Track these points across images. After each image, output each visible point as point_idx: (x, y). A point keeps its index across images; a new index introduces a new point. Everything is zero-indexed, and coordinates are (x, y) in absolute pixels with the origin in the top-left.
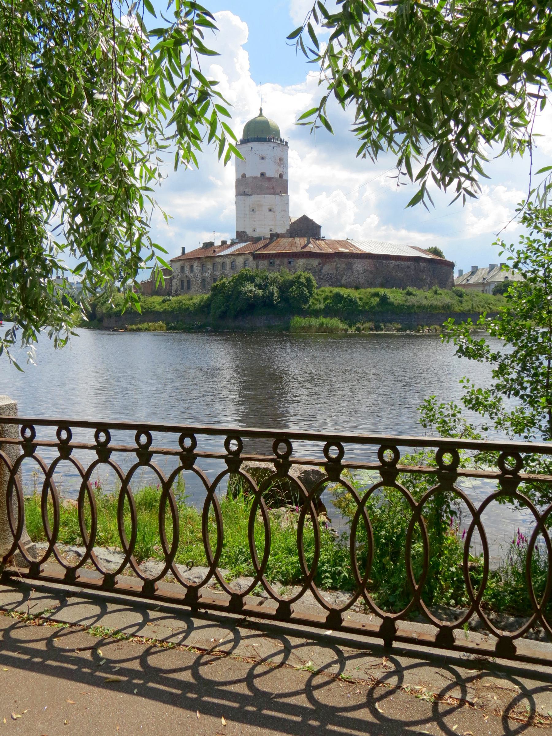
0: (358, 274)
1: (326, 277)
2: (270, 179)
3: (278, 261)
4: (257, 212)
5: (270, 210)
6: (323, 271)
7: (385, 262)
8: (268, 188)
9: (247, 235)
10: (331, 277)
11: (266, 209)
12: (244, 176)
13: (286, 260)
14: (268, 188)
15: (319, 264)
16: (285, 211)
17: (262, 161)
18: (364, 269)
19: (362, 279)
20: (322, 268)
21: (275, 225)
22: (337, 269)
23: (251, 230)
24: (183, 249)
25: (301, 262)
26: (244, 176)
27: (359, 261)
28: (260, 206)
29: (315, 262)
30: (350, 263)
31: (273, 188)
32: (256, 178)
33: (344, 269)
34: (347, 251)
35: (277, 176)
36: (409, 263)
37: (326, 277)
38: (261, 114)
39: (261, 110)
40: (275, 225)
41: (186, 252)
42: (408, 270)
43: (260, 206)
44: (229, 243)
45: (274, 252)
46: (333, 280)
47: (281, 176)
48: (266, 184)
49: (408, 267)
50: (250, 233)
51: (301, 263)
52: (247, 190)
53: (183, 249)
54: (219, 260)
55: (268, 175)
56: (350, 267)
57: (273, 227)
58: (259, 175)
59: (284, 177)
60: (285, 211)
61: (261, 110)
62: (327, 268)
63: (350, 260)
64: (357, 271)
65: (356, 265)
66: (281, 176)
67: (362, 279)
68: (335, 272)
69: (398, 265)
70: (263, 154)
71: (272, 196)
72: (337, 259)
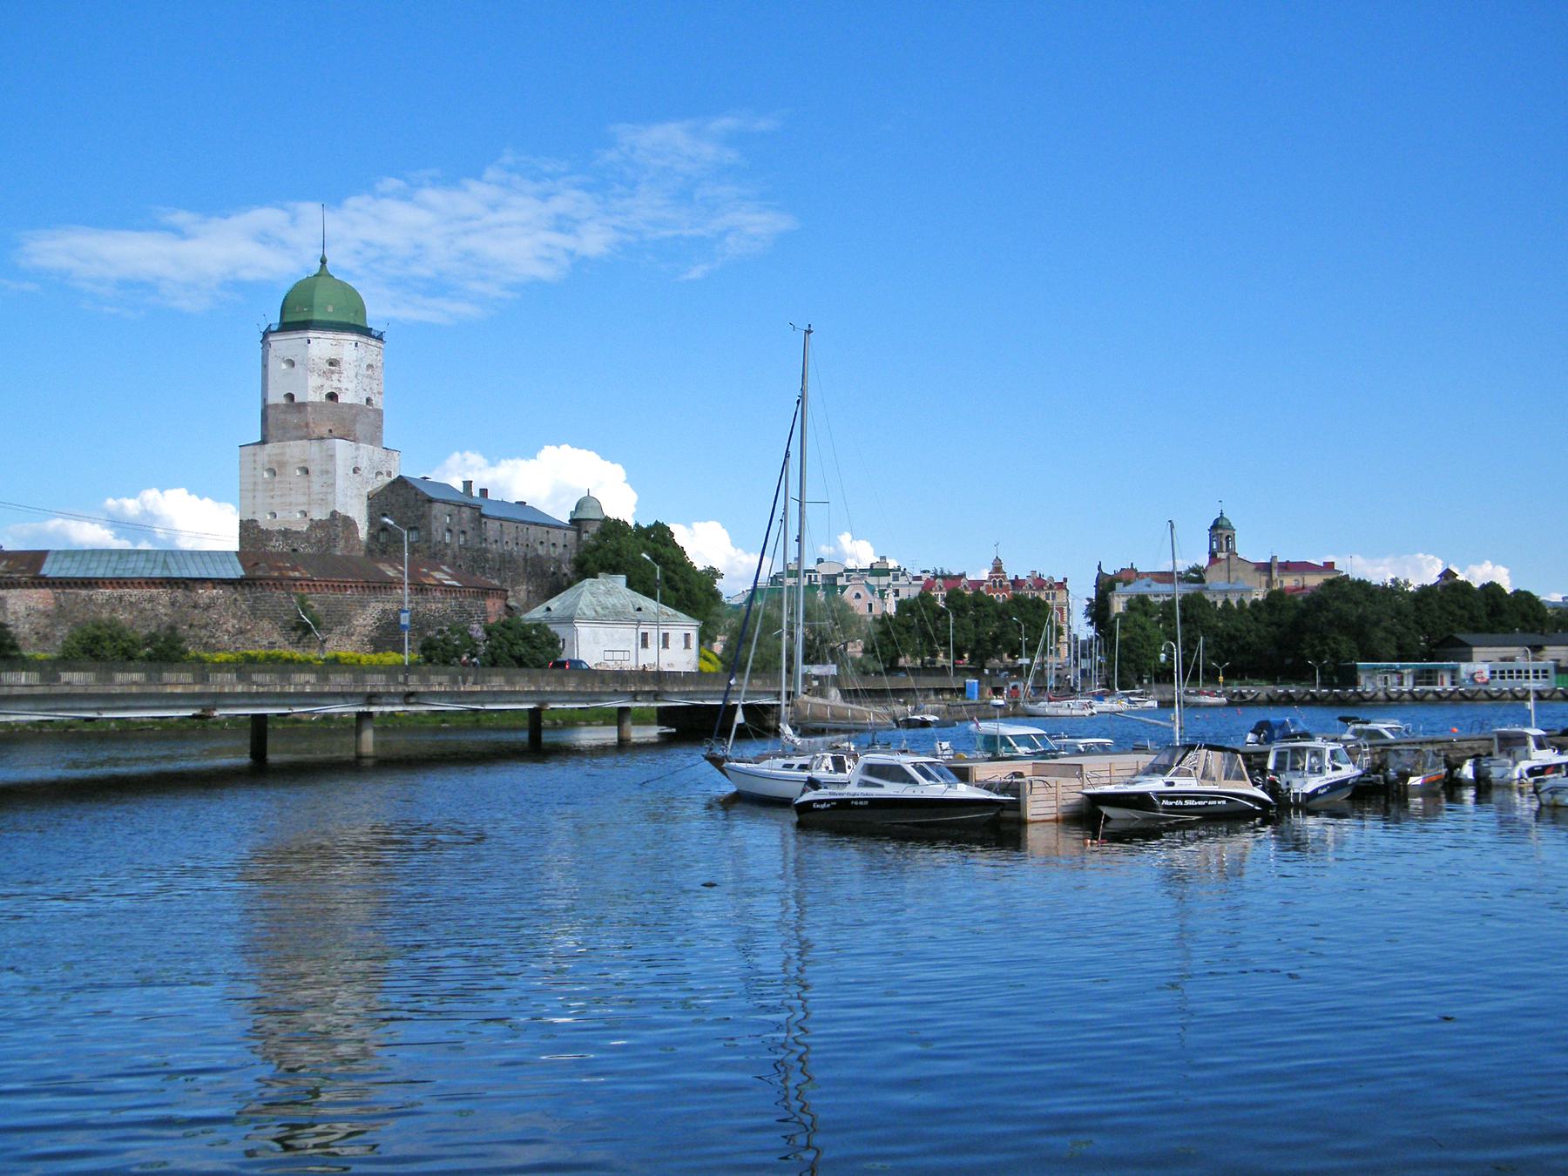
0: (17, 619)
7: (84, 592)
8: (298, 427)
16: (327, 472)
18: (28, 608)
28: (282, 464)
31: (307, 425)
32: (277, 405)
36: (154, 591)
39: (323, 261)
42: (148, 606)
43: (282, 464)
47: (332, 396)
48: (294, 419)
49: (151, 600)
50: (265, 521)
57: (304, 508)
60: (327, 472)
61: (323, 261)
64: (14, 613)
66: (332, 396)
69: (121, 598)
71: (304, 442)
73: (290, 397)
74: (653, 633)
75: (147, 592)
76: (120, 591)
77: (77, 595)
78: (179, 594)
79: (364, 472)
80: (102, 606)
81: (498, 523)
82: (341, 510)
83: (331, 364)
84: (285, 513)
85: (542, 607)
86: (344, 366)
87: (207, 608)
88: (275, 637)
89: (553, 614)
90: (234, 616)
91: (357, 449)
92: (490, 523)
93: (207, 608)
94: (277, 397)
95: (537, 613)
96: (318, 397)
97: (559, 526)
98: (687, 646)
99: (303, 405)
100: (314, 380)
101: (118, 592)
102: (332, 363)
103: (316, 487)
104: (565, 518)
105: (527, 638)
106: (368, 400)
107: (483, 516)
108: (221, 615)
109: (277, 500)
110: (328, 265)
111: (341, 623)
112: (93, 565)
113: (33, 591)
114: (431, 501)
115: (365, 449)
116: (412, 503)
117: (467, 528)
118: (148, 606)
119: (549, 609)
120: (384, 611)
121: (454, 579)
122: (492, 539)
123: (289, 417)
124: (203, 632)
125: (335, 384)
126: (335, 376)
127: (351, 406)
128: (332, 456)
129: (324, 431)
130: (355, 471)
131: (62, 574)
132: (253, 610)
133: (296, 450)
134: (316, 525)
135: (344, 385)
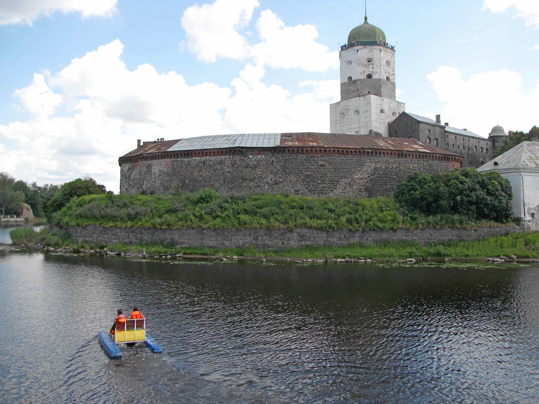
6: (131, 176)
7: (186, 160)
8: (354, 92)
11: (352, 112)
14: (354, 92)
15: (129, 169)
16: (367, 111)
18: (160, 171)
20: (131, 173)
27: (154, 162)
28: (347, 110)
31: (358, 90)
35: (363, 77)
36: (223, 157)
39: (366, 19)
40: (360, 128)
42: (219, 167)
46: (138, 186)
47: (369, 76)
48: (352, 88)
49: (221, 163)
57: (357, 130)
59: (374, 77)
60: (367, 111)
61: (366, 19)
63: (149, 162)
64: (155, 174)
65: (154, 167)
66: (369, 76)
69: (204, 162)
71: (357, 98)
73: (350, 78)
75: (219, 158)
76: (204, 158)
77: (183, 162)
78: (237, 158)
79: (386, 111)
80: (194, 168)
81: (454, 136)
83: (369, 61)
85: (492, 163)
86: (375, 61)
87: (254, 167)
88: (299, 186)
89: (500, 167)
90: (272, 173)
91: (383, 100)
92: (449, 135)
93: (254, 167)
95: (488, 167)
97: (484, 139)
99: (356, 81)
100: (361, 69)
102: (369, 61)
103: (362, 119)
104: (486, 136)
105: (483, 185)
106: (388, 78)
107: (446, 131)
108: (263, 172)
109: (346, 127)
110: (368, 21)
111: (345, 177)
112: (195, 144)
113: (162, 160)
114: (419, 122)
115: (386, 100)
116: (409, 125)
117: (438, 138)
118: (219, 167)
119: (496, 164)
120: (375, 169)
121: (426, 149)
122: (451, 144)
123: (350, 88)
124: (252, 183)
125: (371, 70)
126: (371, 66)
127: (379, 80)
129: (367, 92)
130: (382, 111)
132: (284, 168)
135: (375, 70)
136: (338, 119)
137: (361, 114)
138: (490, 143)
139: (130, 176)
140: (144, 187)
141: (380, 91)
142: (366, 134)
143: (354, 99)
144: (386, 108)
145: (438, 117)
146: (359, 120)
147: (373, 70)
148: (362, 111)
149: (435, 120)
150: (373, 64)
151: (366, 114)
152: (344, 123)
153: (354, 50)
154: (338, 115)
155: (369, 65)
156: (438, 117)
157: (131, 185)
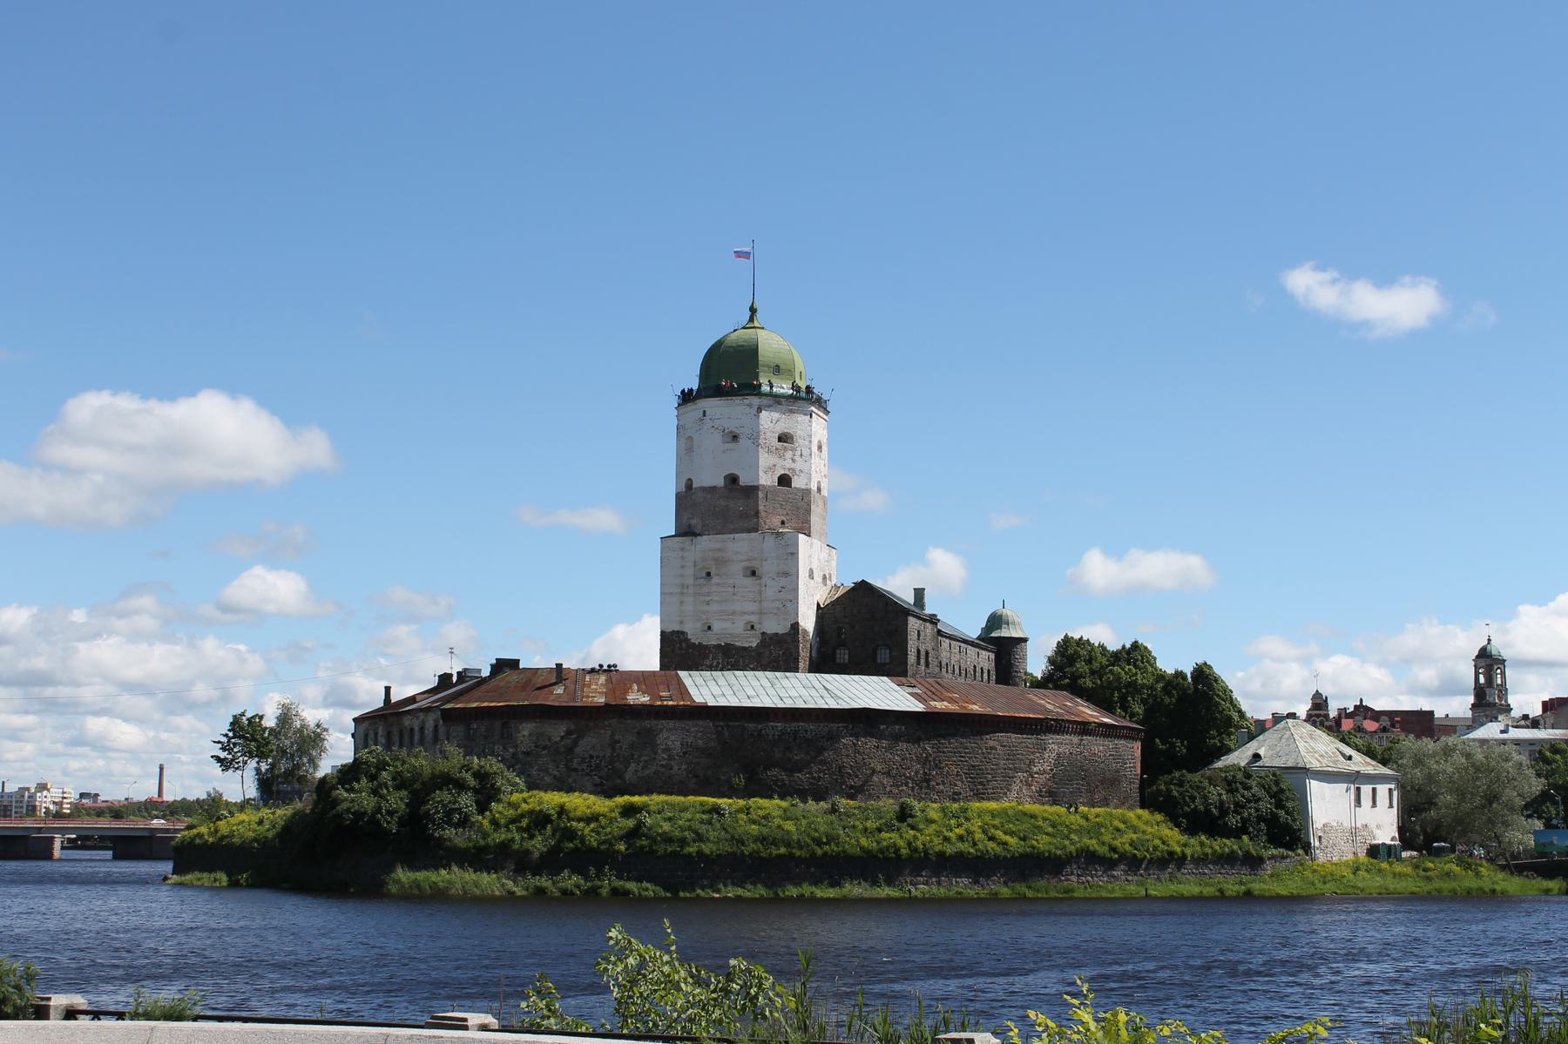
0: (670, 758)
1: (584, 766)
2: (752, 491)
3: (479, 727)
4: (715, 580)
5: (754, 573)
6: (577, 750)
7: (751, 726)
8: (744, 516)
9: (687, 640)
10: (598, 766)
11: (736, 569)
12: (689, 485)
13: (498, 724)
15: (569, 733)
16: (786, 574)
17: (731, 445)
19: (679, 770)
20: (575, 743)
21: (760, 613)
22: (613, 744)
23: (699, 625)
24: (388, 689)
25: (526, 730)
26: (689, 485)
27: (671, 724)
28: (721, 562)
29: (557, 731)
30: (649, 731)
31: (757, 514)
32: (713, 489)
33: (632, 746)
34: (645, 699)
36: (834, 726)
37: (584, 766)
38: (751, 320)
39: (753, 310)
40: (760, 613)
41: (394, 698)
43: (721, 562)
44: (455, 679)
45: (474, 705)
47: (784, 480)
48: (740, 505)
51: (526, 733)
52: (693, 522)
53: (388, 689)
54: (407, 721)
55: (743, 481)
56: (647, 740)
57: (754, 619)
58: (720, 482)
59: (797, 483)
60: (786, 574)
61: (753, 310)
62: (590, 743)
64: (667, 750)
66: (784, 480)
67: (679, 770)
68: (608, 752)
69: (795, 734)
70: (732, 426)
72: (614, 722)
73: (732, 480)
74: (1366, 790)
75: (824, 727)
82: (802, 623)
84: (727, 625)
89: (1266, 762)
94: (711, 477)
96: (767, 480)
97: (972, 644)
98: (1391, 806)
101: (792, 726)
103: (770, 592)
107: (939, 633)
109: (714, 607)
110: (758, 314)
119: (1257, 757)
120: (1059, 754)
126: (789, 454)
128: (794, 555)
130: (811, 576)
131: (722, 702)
133: (739, 545)
134: (769, 640)
135: (799, 465)
136: (690, 581)
137: (765, 580)
138: (992, 656)
139: (570, 750)
140: (628, 776)
141: (808, 522)
142: (781, 632)
143: (744, 535)
144: (814, 567)
145: (919, 593)
146: (760, 593)
147: (793, 466)
148: (768, 569)
149: (912, 601)
150: (794, 450)
151: (783, 581)
152: (708, 594)
153: (750, 405)
154: (690, 571)
155: (785, 449)
156: (919, 593)
157: (575, 770)
